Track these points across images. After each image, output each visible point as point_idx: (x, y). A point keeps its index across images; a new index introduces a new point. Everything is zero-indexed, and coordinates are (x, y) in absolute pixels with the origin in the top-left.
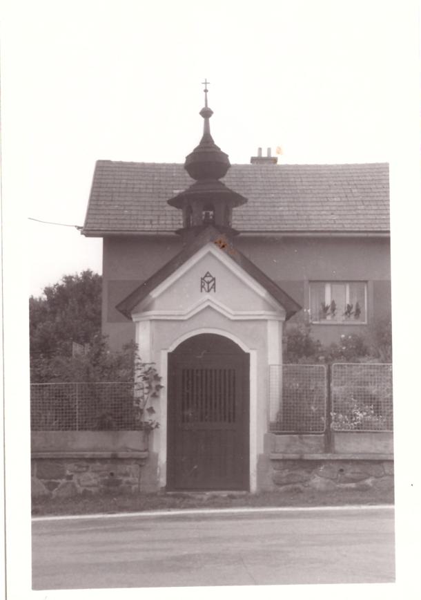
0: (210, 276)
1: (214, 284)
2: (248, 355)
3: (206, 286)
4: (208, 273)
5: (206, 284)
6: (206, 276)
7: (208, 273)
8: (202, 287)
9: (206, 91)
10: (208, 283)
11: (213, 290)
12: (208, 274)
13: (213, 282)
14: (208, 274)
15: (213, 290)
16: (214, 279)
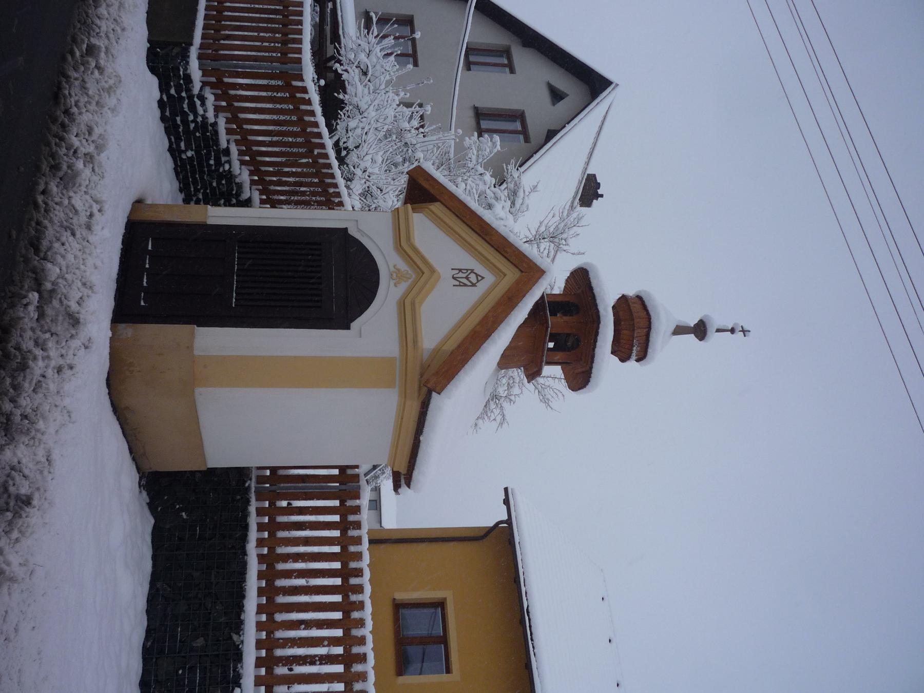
0: (478, 281)
1: (465, 285)
2: (348, 328)
3: (461, 275)
4: (483, 278)
5: (464, 275)
6: (477, 275)
7: (483, 278)
8: (460, 270)
9: (732, 331)
10: (467, 278)
11: (457, 283)
12: (480, 278)
13: (469, 284)
14: (480, 278)
15: (457, 283)
16: (474, 285)
